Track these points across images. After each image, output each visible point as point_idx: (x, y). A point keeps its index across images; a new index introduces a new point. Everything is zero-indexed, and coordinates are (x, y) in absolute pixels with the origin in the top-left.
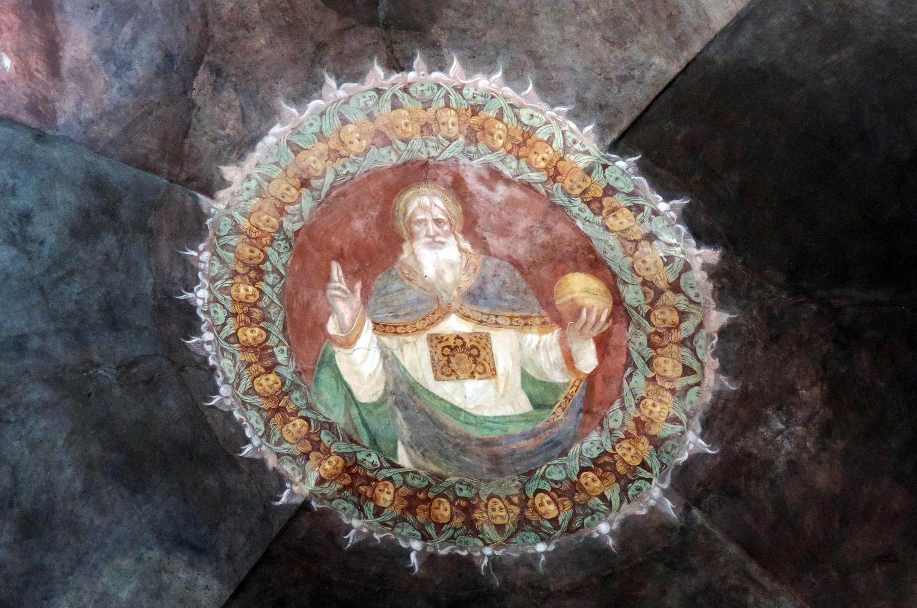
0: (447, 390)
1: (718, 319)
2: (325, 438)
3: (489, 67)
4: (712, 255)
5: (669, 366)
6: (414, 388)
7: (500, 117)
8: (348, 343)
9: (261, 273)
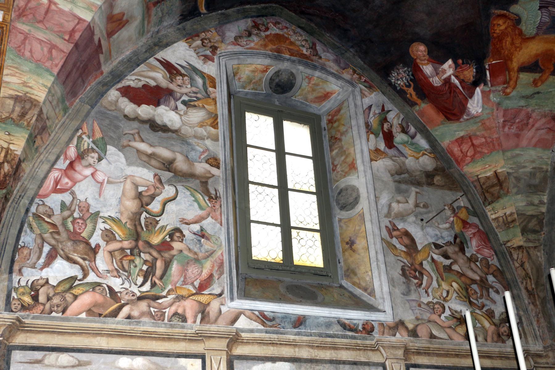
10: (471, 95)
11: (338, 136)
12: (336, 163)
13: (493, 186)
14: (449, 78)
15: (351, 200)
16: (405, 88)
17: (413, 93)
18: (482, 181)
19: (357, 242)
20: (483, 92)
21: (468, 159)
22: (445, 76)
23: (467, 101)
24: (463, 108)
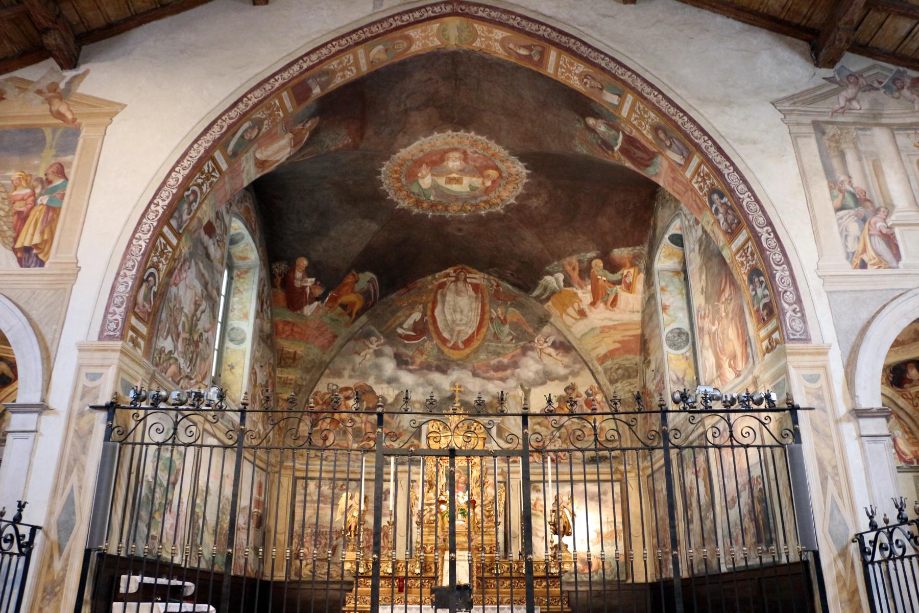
0: (449, 186)
1: (525, 181)
2: (412, 195)
3: (483, 135)
4: (529, 172)
5: (510, 187)
6: (439, 186)
7: (482, 143)
8: (423, 177)
9: (402, 165)
10: (311, 303)
11: (241, 289)
12: (235, 307)
13: (289, 358)
14: (306, 287)
15: (239, 338)
16: (277, 275)
17: (279, 281)
18: (284, 352)
19: (237, 368)
20: (318, 306)
21: (284, 335)
22: (305, 284)
23: (306, 305)
24: (301, 307)
